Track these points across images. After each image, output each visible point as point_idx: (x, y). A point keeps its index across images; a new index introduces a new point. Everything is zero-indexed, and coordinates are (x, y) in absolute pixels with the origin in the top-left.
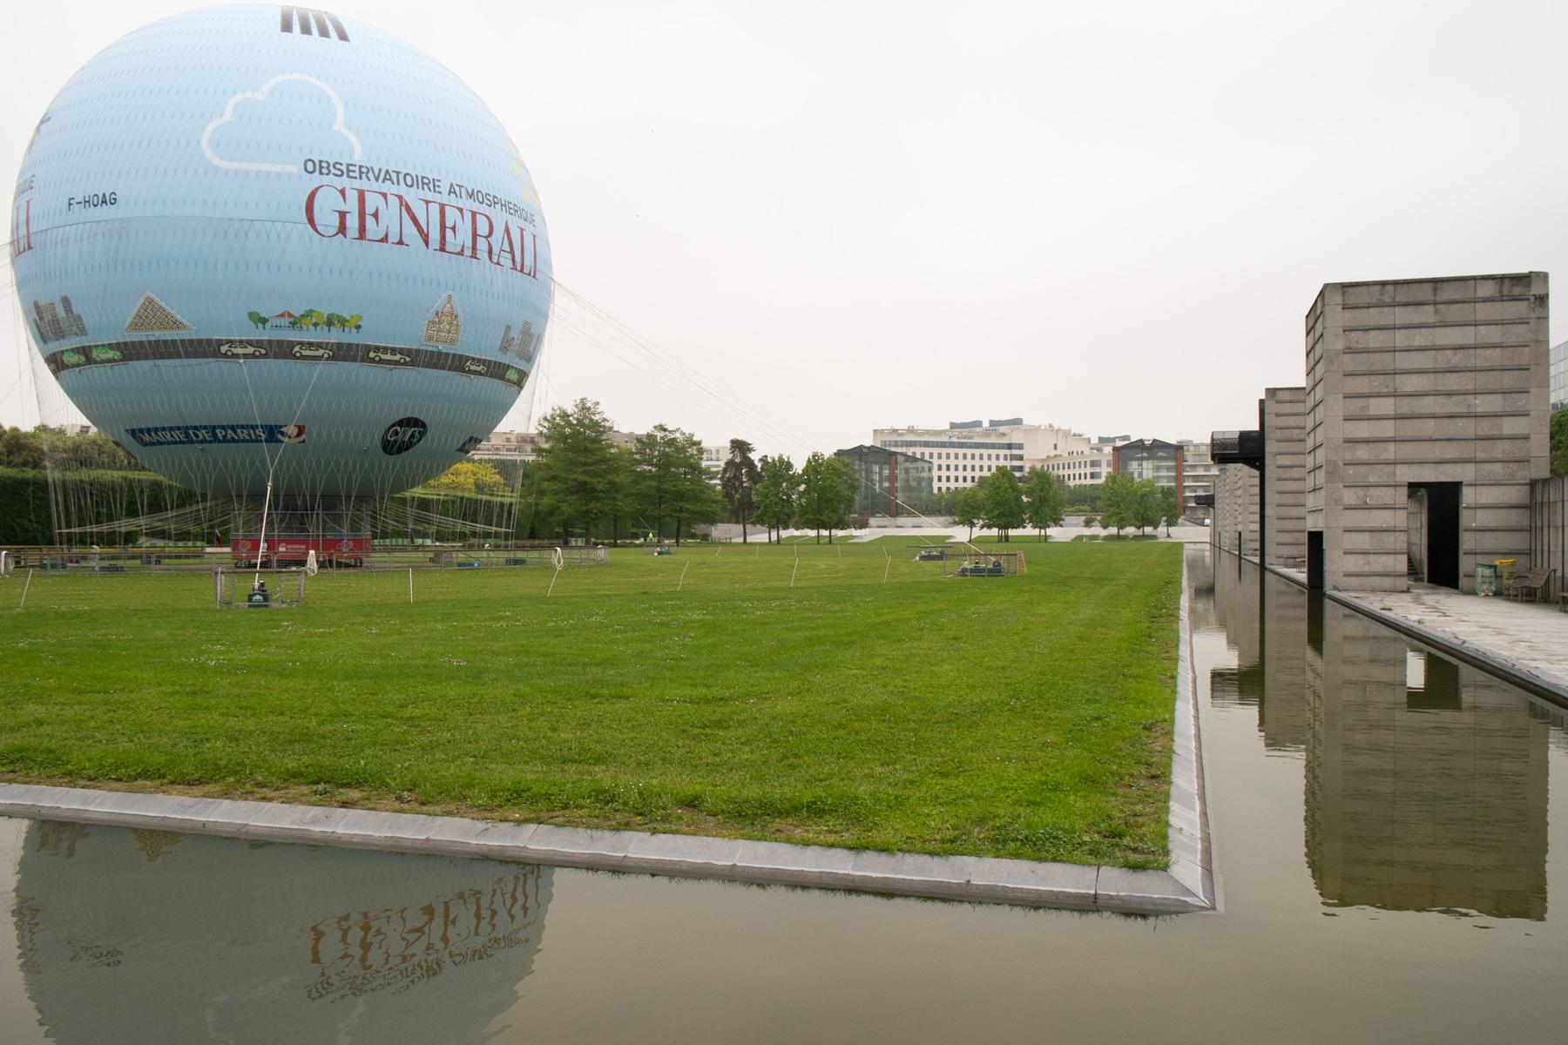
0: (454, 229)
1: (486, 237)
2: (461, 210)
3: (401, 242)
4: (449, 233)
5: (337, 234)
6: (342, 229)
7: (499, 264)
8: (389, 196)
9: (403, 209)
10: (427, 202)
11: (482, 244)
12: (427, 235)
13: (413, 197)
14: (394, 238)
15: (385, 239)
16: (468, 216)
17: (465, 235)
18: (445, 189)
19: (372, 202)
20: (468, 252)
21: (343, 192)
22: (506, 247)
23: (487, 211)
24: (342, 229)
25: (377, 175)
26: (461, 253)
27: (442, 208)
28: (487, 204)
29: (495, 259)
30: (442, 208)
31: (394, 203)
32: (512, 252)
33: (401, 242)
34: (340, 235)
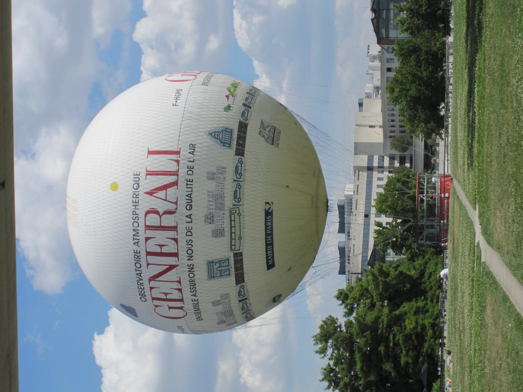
0: (161, 246)
1: (160, 217)
2: (147, 239)
3: (179, 282)
4: (165, 250)
5: (183, 310)
6: (181, 308)
7: (176, 203)
8: (151, 286)
9: (156, 280)
10: (148, 264)
11: (168, 220)
12: (170, 266)
13: (148, 273)
14: (176, 285)
15: (180, 290)
16: (150, 234)
17: (161, 237)
18: (136, 248)
19: (156, 293)
20: (172, 234)
21: (156, 306)
22: (161, 194)
23: (142, 216)
24: (181, 308)
25: (139, 279)
26: (176, 240)
27: (149, 254)
28: (138, 220)
29: (172, 207)
30: (149, 254)
31: (153, 284)
32: (165, 187)
33: (179, 282)
34: (183, 308)
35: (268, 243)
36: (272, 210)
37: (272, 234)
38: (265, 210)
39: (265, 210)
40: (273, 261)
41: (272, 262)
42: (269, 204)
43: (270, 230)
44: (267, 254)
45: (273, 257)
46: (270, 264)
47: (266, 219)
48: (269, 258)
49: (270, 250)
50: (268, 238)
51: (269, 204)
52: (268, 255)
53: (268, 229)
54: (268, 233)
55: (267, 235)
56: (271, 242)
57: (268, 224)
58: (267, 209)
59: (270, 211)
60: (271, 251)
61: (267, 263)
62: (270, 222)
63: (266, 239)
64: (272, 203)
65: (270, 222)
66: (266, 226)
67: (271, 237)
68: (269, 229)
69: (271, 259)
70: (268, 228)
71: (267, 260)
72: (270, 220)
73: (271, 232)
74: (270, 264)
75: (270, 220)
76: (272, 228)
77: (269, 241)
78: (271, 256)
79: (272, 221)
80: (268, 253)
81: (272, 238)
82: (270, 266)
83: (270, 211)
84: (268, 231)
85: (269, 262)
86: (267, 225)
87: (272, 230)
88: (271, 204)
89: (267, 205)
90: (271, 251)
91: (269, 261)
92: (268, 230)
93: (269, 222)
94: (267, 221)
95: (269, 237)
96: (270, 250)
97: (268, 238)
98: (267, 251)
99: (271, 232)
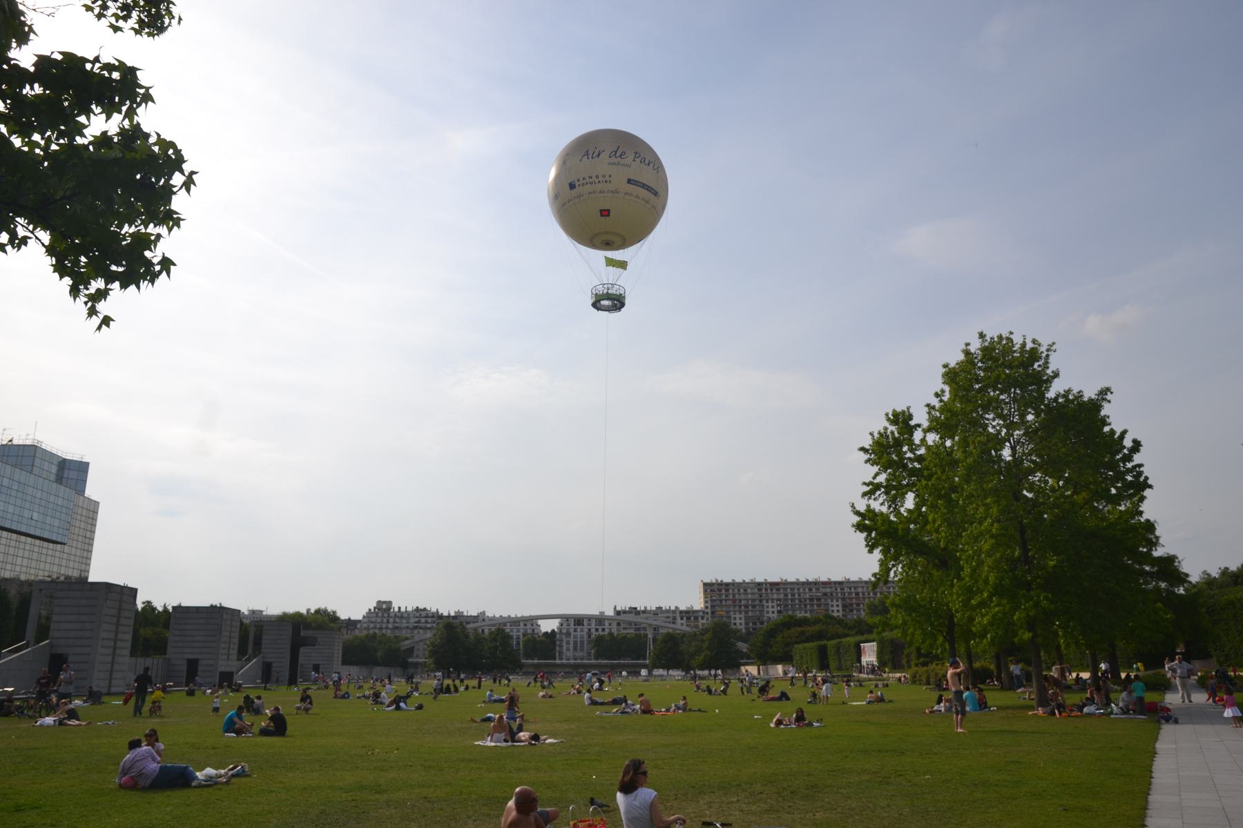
37: (648, 190)
55: (649, 187)
66: (652, 189)
71: (635, 181)
82: (629, 181)
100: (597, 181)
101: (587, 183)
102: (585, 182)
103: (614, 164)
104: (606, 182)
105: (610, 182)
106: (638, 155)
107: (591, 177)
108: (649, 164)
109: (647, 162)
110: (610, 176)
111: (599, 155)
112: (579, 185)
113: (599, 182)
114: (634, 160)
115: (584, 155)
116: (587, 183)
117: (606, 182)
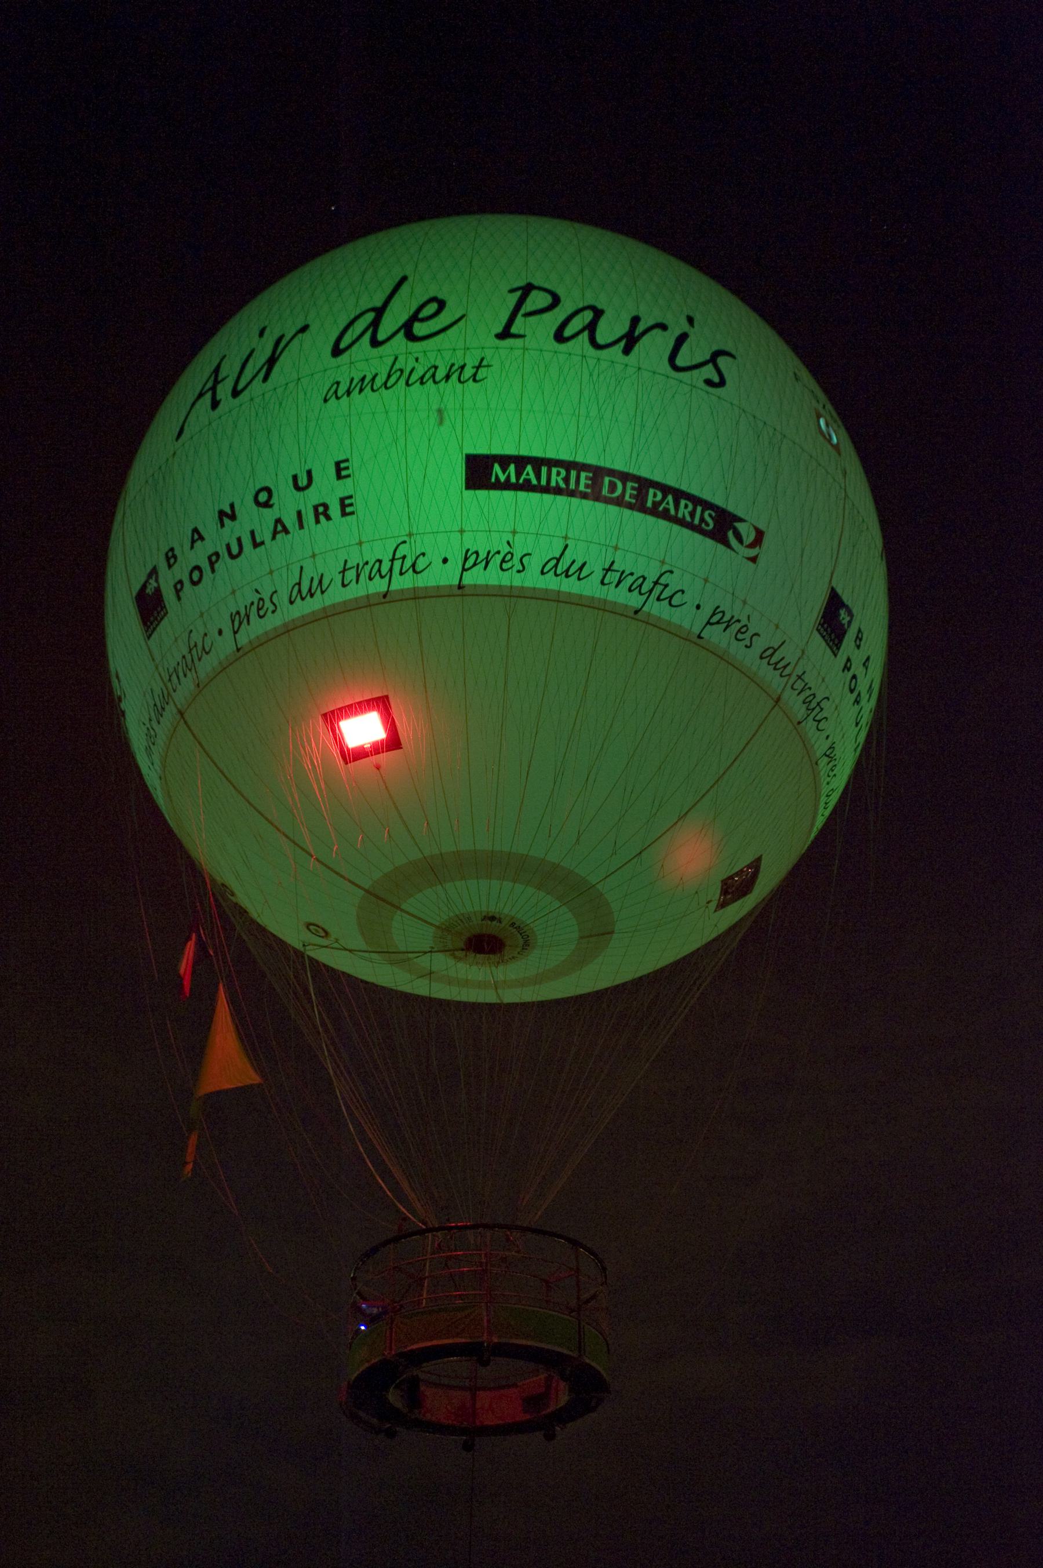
35: (607, 480)
36: (727, 545)
38: (741, 520)
39: (741, 520)
40: (507, 486)
41: (502, 478)
42: (752, 546)
43: (656, 505)
44: (551, 463)
45: (527, 487)
46: (497, 468)
47: (707, 505)
48: (529, 468)
49: (566, 480)
50: (629, 484)
51: (752, 546)
52: (544, 470)
53: (664, 497)
54: (651, 491)
56: (605, 491)
57: (686, 506)
58: (739, 525)
59: (730, 534)
60: (562, 485)
61: (505, 461)
62: (688, 519)
63: (625, 477)
64: (754, 560)
65: (688, 519)
66: (679, 495)
67: (627, 498)
68: (660, 503)
69: (518, 477)
70: (670, 498)
71: (521, 462)
72: (697, 521)
73: (649, 504)
74: (497, 468)
75: (697, 521)
76: (665, 515)
77: (613, 487)
78: (534, 482)
79: (690, 526)
80: (554, 470)
81: (619, 502)
83: (730, 534)
84: (655, 495)
85: (504, 470)
86: (683, 502)
87: (654, 511)
88: (752, 553)
89: (752, 536)
90: (562, 485)
91: (512, 468)
92: (659, 496)
93: (692, 514)
94: (699, 509)
95: (629, 492)
96: (566, 480)
97: (629, 484)
98: (569, 466)
99: (649, 504)
100: (263, 522)
101: (213, 559)
102: (199, 556)
103: (365, 384)
104: (322, 512)
105: (345, 506)
106: (538, 300)
107: (227, 515)
108: (630, 341)
109: (609, 330)
110: (340, 470)
111: (272, 361)
112: (179, 585)
113: (280, 527)
114: (505, 334)
115: (201, 395)
116: (213, 559)
117: (322, 512)
